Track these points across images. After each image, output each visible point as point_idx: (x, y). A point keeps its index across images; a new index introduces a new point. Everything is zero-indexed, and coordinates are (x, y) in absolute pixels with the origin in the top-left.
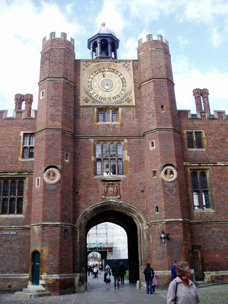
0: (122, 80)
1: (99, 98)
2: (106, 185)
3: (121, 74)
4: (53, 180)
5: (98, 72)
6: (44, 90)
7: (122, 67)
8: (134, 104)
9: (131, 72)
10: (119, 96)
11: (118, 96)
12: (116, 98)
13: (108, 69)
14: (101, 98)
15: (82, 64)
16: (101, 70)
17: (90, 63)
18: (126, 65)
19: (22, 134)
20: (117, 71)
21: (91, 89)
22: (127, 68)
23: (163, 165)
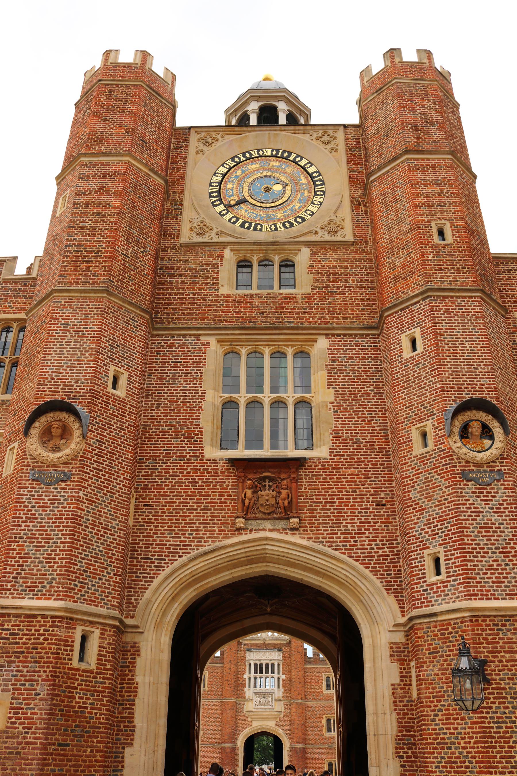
0: (312, 178)
1: (242, 226)
2: (249, 482)
3: (310, 163)
4: (56, 449)
5: (240, 159)
6: (68, 192)
7: (315, 143)
8: (349, 237)
10: (303, 220)
11: (299, 220)
12: (292, 225)
13: (273, 150)
14: (247, 225)
15: (194, 138)
16: (251, 154)
17: (219, 137)
20: (298, 156)
21: (219, 202)
22: (332, 145)
23: (453, 406)
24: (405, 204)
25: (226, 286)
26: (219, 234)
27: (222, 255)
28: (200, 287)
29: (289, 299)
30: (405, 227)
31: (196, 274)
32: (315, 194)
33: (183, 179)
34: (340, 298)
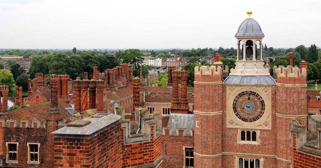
8: (270, 129)
9: (270, 96)
18: (266, 89)
19: (184, 148)
20: (258, 94)
24: (284, 131)
25: (239, 141)
26: (237, 124)
27: (237, 131)
28: (232, 141)
29: (254, 146)
30: (284, 139)
31: (231, 137)
32: (262, 109)
33: (226, 104)
34: (267, 147)
